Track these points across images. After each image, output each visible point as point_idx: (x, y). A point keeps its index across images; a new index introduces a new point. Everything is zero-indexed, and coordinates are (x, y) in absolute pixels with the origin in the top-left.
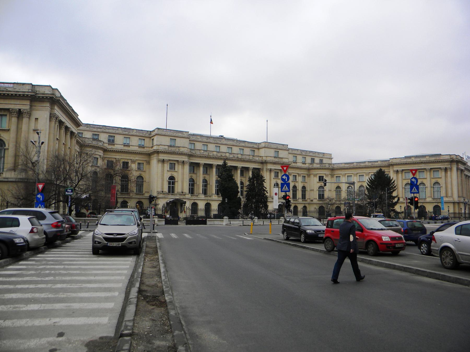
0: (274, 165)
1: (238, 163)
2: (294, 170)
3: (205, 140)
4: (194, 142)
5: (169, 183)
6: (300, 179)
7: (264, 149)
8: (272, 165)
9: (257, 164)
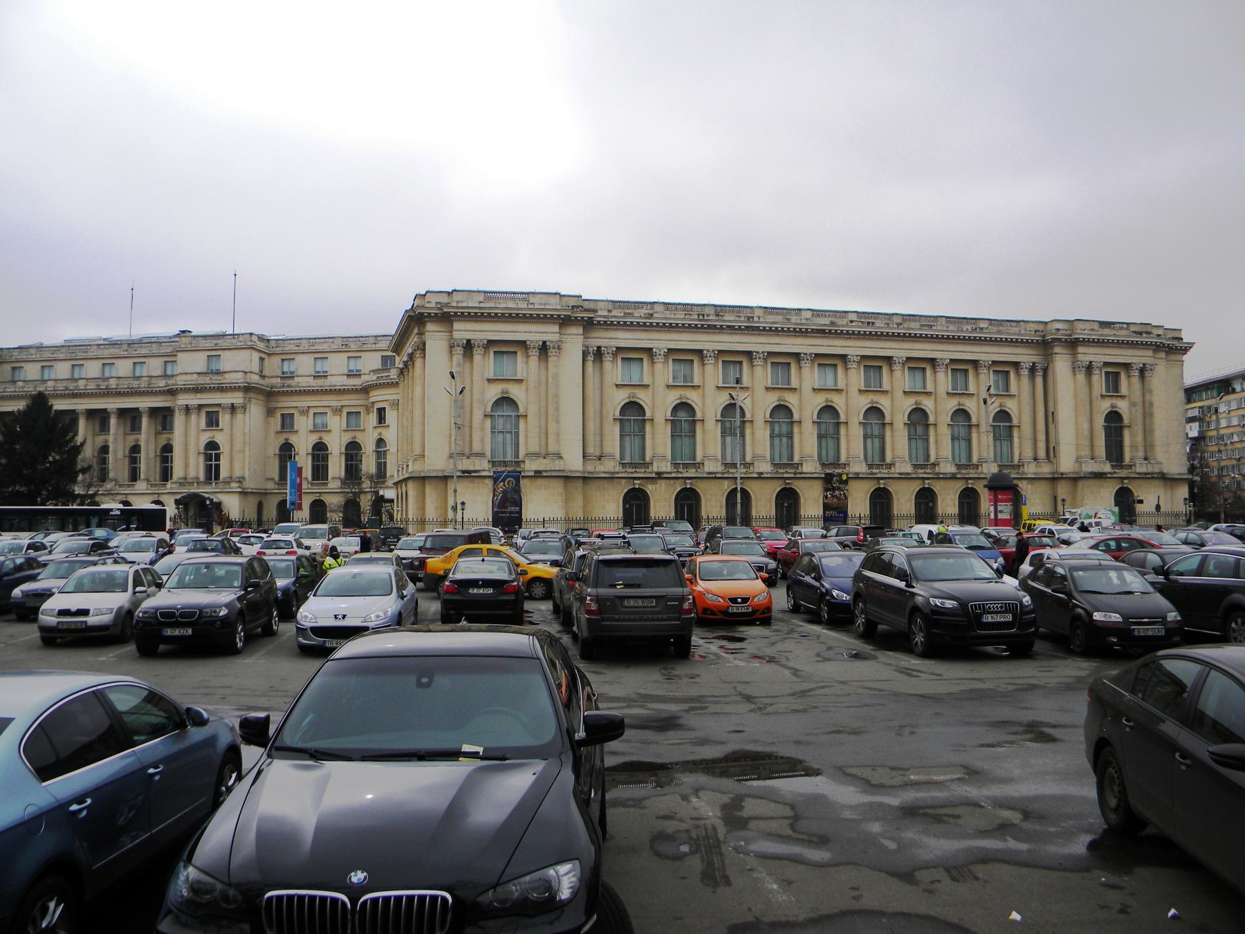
0: (199, 395)
1: (110, 400)
2: (319, 398)
3: (47, 355)
4: (22, 364)
5: (208, 458)
6: (336, 423)
7: (247, 352)
8: (192, 396)
9: (161, 398)
